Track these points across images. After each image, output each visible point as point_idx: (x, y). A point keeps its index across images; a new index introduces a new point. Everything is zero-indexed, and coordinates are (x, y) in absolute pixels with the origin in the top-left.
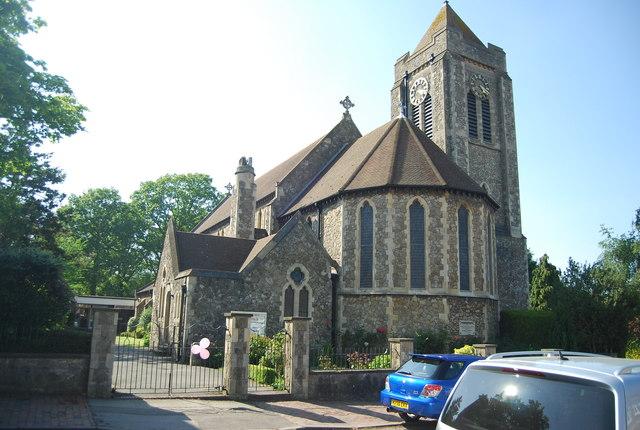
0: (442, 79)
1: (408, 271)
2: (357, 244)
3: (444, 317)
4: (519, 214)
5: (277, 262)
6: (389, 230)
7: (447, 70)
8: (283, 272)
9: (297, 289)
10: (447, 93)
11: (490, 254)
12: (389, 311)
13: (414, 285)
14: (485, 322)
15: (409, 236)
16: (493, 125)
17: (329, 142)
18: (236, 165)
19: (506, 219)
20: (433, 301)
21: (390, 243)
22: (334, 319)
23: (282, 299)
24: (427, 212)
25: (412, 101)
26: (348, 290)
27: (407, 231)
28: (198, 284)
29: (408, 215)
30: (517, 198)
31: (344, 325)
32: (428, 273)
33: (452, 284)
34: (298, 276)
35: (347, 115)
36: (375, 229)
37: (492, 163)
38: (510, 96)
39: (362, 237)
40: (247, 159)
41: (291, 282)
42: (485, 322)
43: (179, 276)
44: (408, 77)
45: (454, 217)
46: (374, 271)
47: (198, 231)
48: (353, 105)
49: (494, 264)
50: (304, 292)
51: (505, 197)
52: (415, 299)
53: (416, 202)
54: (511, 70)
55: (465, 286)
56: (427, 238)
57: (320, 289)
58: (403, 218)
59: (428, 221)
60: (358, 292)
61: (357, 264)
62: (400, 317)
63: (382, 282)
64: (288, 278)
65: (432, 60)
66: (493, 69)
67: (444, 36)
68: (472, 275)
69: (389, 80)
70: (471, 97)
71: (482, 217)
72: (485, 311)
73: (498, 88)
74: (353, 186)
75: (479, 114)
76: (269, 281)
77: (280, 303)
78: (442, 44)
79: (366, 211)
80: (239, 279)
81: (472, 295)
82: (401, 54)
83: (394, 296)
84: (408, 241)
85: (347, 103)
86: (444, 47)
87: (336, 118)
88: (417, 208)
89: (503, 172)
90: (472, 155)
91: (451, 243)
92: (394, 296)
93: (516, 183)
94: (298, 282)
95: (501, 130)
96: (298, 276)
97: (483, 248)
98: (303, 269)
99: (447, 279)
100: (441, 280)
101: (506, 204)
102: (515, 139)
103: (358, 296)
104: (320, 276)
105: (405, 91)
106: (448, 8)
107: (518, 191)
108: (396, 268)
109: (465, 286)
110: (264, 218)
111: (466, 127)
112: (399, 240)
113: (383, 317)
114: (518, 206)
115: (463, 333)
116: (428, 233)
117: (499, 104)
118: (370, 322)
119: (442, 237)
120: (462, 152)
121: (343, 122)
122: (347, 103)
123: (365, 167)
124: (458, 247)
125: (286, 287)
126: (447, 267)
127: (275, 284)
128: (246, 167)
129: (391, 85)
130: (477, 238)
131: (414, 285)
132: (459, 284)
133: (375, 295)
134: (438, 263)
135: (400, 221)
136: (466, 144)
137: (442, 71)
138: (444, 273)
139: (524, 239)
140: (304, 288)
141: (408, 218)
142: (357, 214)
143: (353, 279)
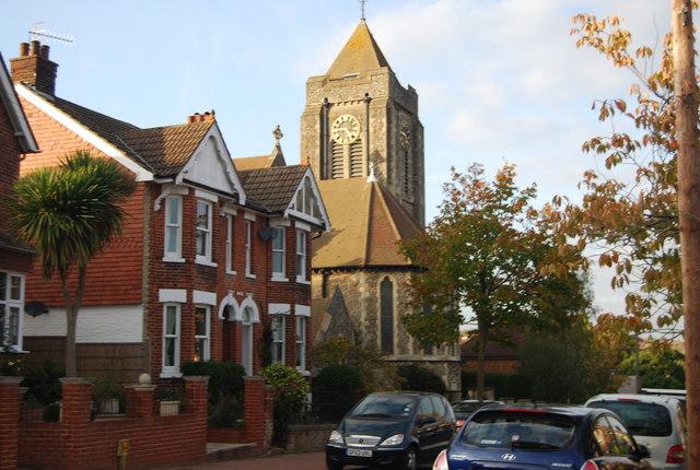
2: (379, 315)
7: (389, 122)
16: (410, 176)
39: (383, 308)
44: (329, 105)
46: (396, 340)
52: (428, 364)
61: (379, 333)
63: (403, 350)
79: (387, 285)
85: (278, 133)
122: (278, 133)
123: (375, 239)
137: (384, 120)
142: (378, 288)
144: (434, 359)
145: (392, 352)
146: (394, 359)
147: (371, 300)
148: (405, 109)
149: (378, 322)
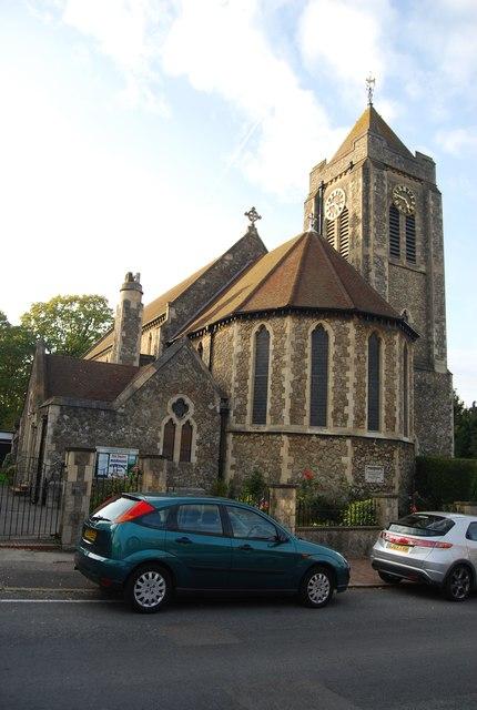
0: (361, 190)
1: (307, 407)
3: (346, 460)
4: (445, 347)
5: (156, 392)
6: (287, 358)
7: (366, 180)
8: (163, 403)
9: (179, 424)
10: (366, 206)
11: (405, 391)
12: (284, 452)
13: (313, 423)
14: (396, 467)
15: (309, 367)
16: (418, 243)
17: (231, 258)
18: (122, 281)
19: (430, 352)
20: (335, 442)
21: (287, 372)
22: (222, 461)
23: (161, 435)
24: (332, 339)
25: (326, 215)
26: (237, 426)
27: (308, 361)
28: (62, 415)
29: (309, 342)
30: (443, 329)
31: (233, 467)
32: (331, 409)
33: (358, 424)
34: (180, 408)
35: (252, 228)
36: (271, 357)
37: (415, 287)
38: (439, 211)
40: (134, 274)
41: (173, 416)
42: (396, 467)
43: (44, 404)
44: (324, 187)
45: (363, 346)
46: (269, 405)
47: (87, 358)
48: (260, 218)
49: (411, 402)
50: (187, 428)
51: (429, 326)
52: (314, 438)
53: (320, 327)
54: (440, 183)
55: (374, 426)
56: (330, 369)
57: (207, 425)
58: (304, 345)
59: (332, 350)
60: (249, 429)
62: (296, 459)
63: (277, 419)
64: (169, 410)
65: (351, 168)
66: (420, 180)
67: (364, 141)
68: (383, 413)
69: (305, 189)
70: (394, 211)
71: (397, 347)
72: (396, 454)
73: (425, 203)
74: (254, 306)
75: (403, 231)
76: (146, 413)
77: (158, 440)
78: (361, 152)
79: (262, 335)
80: (113, 412)
81: (381, 436)
82: (319, 161)
83: (289, 434)
84: (308, 371)
85: (253, 214)
86: (365, 154)
87: (238, 232)
88: (320, 335)
89: (428, 299)
90: (392, 278)
91: (359, 376)
92: (289, 434)
93: (442, 311)
94: (180, 416)
95: (427, 250)
96: (180, 408)
97: (397, 382)
98: (187, 401)
99: (352, 417)
100: (345, 419)
101: (429, 334)
102: (443, 260)
103: (249, 433)
104: (206, 408)
105: (319, 201)
106: (372, 111)
107: (444, 320)
108: (294, 403)
109: (374, 426)
110: (150, 343)
111: (387, 245)
112: (298, 371)
113: (278, 459)
114: (444, 338)
115: (369, 480)
116: (332, 364)
117: (425, 220)
118: (262, 464)
119: (348, 369)
120: (380, 273)
121: (247, 236)
122: (253, 214)
123: (267, 285)
124: (366, 380)
125: (166, 421)
126: (352, 403)
127: (153, 417)
128: (133, 284)
129: (306, 197)
130: (390, 370)
131: (313, 423)
132: (366, 422)
133: (268, 433)
134: (343, 398)
135: (300, 348)
136: (386, 264)
137: (361, 180)
138: (349, 410)
139: (449, 374)
140: (188, 422)
141: (310, 345)
142: (252, 340)
143: (246, 415)
144: (328, 433)
145: (264, 422)
146: (266, 429)
147: (243, 356)
148: (391, 167)
149: (250, 383)
